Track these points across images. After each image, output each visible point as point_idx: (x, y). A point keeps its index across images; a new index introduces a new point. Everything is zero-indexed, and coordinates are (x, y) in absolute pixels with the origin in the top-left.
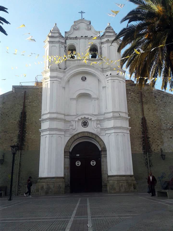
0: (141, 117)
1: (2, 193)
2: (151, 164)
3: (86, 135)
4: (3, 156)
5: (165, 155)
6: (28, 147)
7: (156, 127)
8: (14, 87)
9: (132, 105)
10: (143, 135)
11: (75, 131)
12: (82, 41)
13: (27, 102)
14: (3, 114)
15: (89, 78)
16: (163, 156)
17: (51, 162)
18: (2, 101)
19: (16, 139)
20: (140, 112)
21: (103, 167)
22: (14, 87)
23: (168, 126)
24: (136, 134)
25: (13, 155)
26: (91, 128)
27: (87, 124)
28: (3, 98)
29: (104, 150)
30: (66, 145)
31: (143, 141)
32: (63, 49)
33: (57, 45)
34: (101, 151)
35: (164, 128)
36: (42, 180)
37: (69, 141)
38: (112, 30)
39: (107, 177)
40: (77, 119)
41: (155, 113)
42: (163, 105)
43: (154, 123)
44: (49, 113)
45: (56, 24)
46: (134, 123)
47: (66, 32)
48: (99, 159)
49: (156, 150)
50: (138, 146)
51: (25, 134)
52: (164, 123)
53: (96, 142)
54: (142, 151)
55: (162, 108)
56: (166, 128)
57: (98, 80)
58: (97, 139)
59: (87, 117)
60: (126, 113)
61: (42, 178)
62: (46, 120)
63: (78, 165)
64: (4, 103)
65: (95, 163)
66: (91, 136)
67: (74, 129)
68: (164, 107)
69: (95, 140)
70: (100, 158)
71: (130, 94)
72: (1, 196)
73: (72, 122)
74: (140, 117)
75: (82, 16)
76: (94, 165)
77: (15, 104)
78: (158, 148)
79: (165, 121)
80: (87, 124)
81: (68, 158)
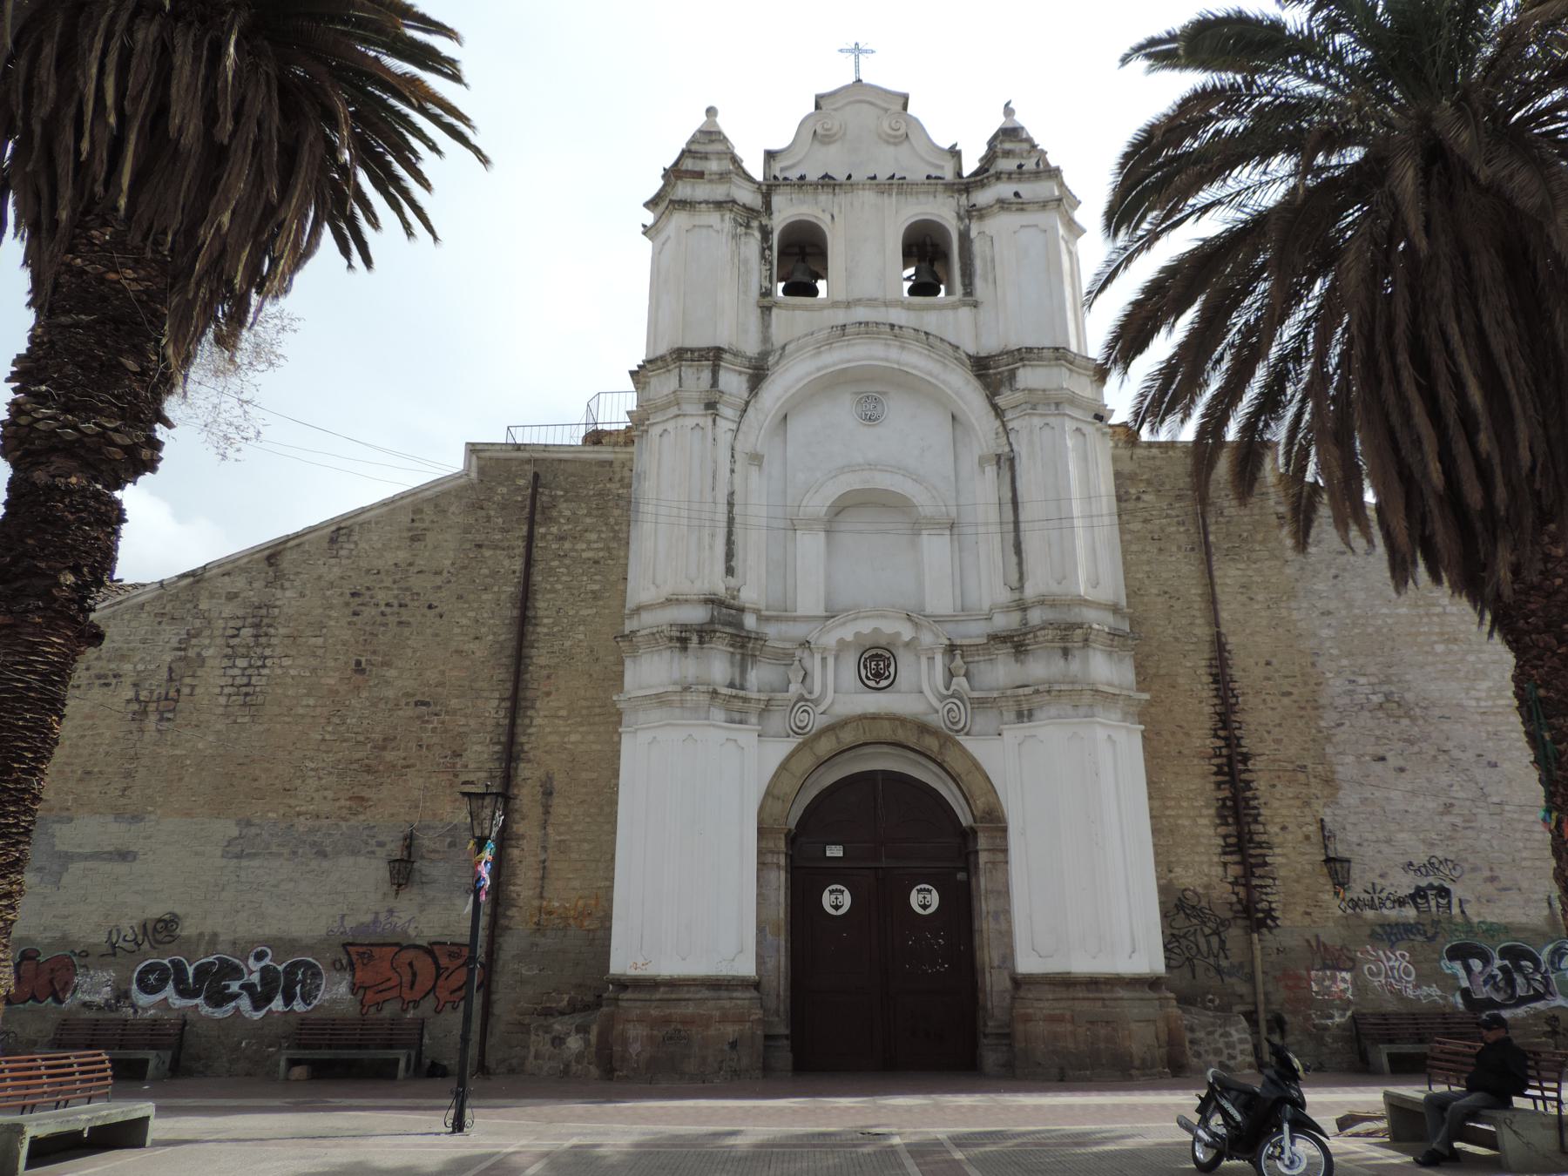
0: (1203, 631)
1: (397, 1061)
2: (1263, 911)
3: (885, 731)
5: (1348, 861)
6: (551, 794)
7: (1290, 694)
8: (473, 449)
9: (1149, 562)
10: (1221, 743)
11: (822, 708)
13: (544, 536)
14: (407, 600)
15: (898, 410)
16: (1338, 866)
17: (688, 885)
18: (410, 530)
19: (478, 748)
20: (1196, 606)
21: (985, 926)
22: (473, 449)
23: (1359, 689)
24: (1173, 733)
26: (918, 691)
27: (892, 669)
28: (414, 512)
29: (995, 821)
30: (769, 794)
31: (1216, 774)
32: (752, 245)
33: (721, 223)
35: (1339, 702)
37: (784, 766)
38: (1026, 146)
39: (1008, 984)
40: (831, 639)
41: (1284, 613)
42: (1329, 567)
43: (1277, 671)
45: (711, 112)
46: (1162, 672)
47: (770, 156)
48: (961, 876)
49: (1292, 827)
50: (1185, 804)
51: (531, 718)
52: (1339, 673)
53: (943, 775)
54: (1211, 832)
55: (1320, 587)
56: (1347, 700)
58: (951, 759)
60: (1115, 609)
63: (837, 907)
65: (934, 899)
66: (912, 740)
67: (816, 694)
68: (1336, 577)
69: (940, 765)
70: (966, 869)
71: (1138, 499)
72: (392, 1076)
74: (1197, 631)
75: (857, 70)
77: (479, 546)
78: (1308, 819)
79: (1345, 662)
80: (892, 669)
81: (778, 866)
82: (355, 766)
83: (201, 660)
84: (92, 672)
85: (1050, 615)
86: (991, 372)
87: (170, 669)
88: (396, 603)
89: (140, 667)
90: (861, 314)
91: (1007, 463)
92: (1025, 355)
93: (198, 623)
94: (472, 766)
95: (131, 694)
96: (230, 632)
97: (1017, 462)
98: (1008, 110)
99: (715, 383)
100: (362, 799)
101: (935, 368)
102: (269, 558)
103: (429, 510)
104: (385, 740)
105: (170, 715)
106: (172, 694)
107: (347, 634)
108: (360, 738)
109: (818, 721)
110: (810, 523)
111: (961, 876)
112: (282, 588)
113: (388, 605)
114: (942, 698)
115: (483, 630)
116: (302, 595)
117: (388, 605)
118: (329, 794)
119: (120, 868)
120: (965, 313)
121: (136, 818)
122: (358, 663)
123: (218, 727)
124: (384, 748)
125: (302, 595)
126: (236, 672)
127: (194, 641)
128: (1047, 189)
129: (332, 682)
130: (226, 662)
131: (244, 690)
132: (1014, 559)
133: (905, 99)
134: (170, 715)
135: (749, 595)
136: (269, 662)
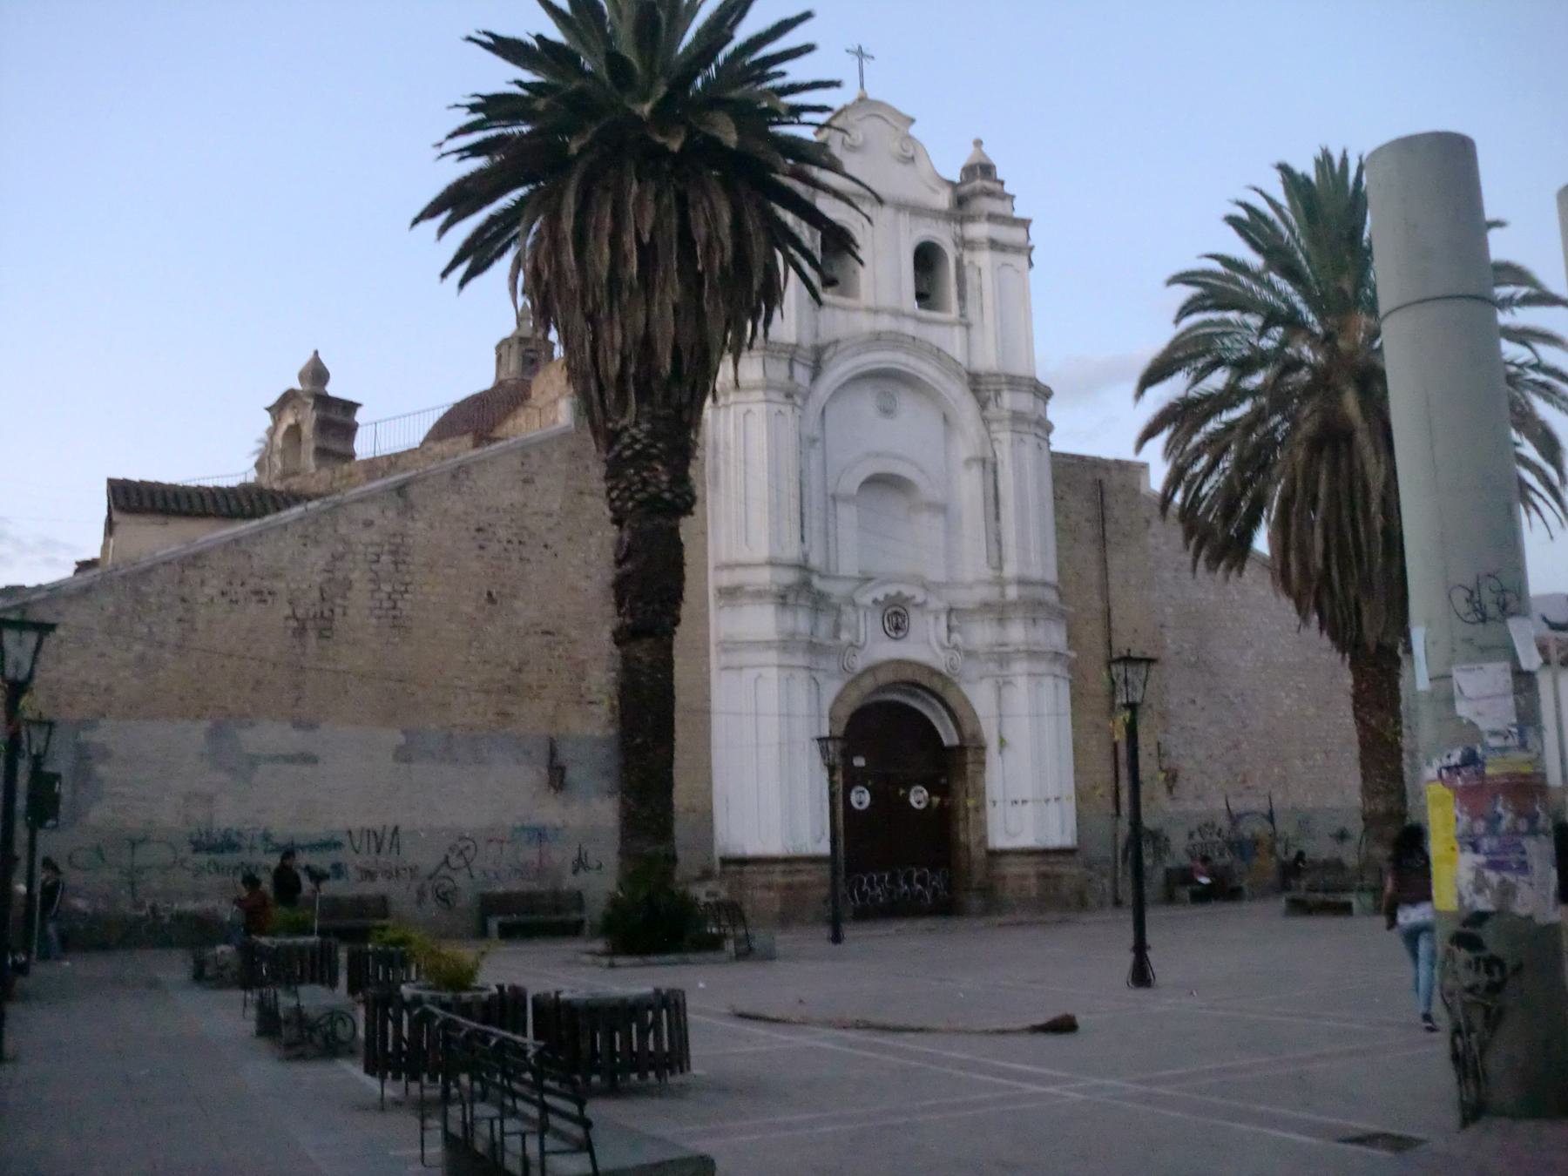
0: (1098, 604)
3: (908, 674)
4: (553, 753)
12: (883, 215)
14: (525, 539)
25: (826, 774)
26: (924, 646)
34: (961, 749)
36: (747, 868)
37: (839, 699)
39: (983, 853)
40: (866, 599)
44: (772, 563)
57: (940, 421)
59: (907, 591)
61: (743, 861)
62: (759, 595)
64: (526, 481)
73: (848, 609)
76: (922, 806)
77: (581, 493)
83: (349, 585)
84: (248, 588)
85: (1029, 591)
86: (976, 382)
87: (322, 591)
88: (515, 540)
89: (293, 586)
90: (885, 323)
91: (989, 466)
92: (1015, 382)
93: (340, 548)
94: (594, 688)
95: (288, 611)
97: (999, 467)
98: (978, 143)
99: (791, 377)
101: (942, 379)
102: (401, 489)
103: (535, 455)
106: (327, 613)
109: (860, 663)
110: (847, 499)
111: (943, 781)
112: (413, 518)
113: (509, 542)
114: (943, 648)
115: (593, 570)
116: (432, 526)
117: (509, 542)
119: (306, 770)
120: (958, 332)
121: (312, 726)
122: (490, 594)
125: (432, 526)
127: (338, 564)
128: (1016, 235)
129: (470, 610)
130: (371, 586)
132: (994, 548)
133: (912, 121)
135: (815, 560)
136: (410, 588)
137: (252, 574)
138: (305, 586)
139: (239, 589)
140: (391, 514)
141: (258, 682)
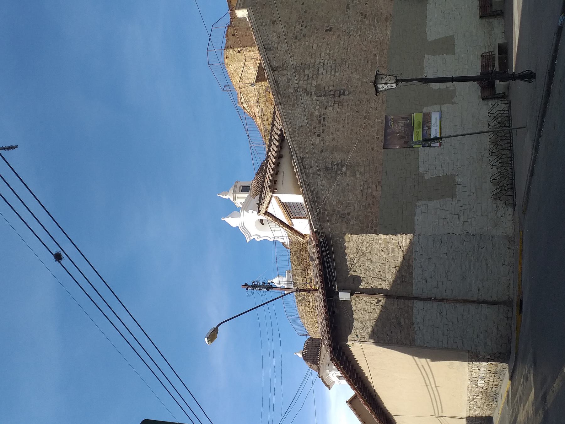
82: (372, 23)
84: (317, 126)
87: (320, 96)
95: (330, 108)
96: (306, 78)
100: (387, 18)
104: (362, 15)
105: (342, 92)
106: (332, 93)
107: (313, 37)
108: (360, 23)
116: (293, 56)
118: (383, 29)
122: (327, 31)
123: (350, 72)
124: (366, 15)
126: (325, 71)
127: (308, 90)
131: (333, 67)
134: (342, 92)
137: (311, 125)
138: (318, 103)
139: (317, 129)
140: (285, 72)
141: (365, 118)
